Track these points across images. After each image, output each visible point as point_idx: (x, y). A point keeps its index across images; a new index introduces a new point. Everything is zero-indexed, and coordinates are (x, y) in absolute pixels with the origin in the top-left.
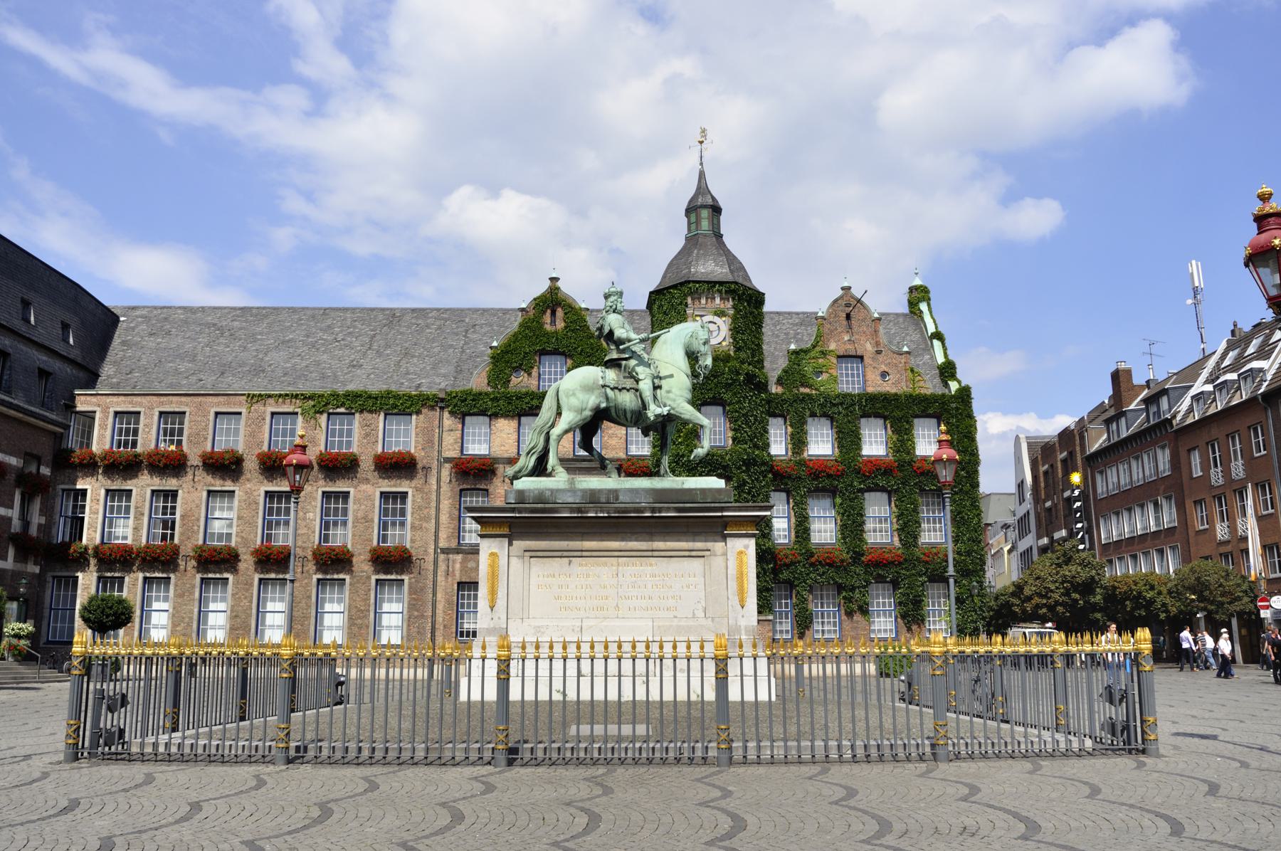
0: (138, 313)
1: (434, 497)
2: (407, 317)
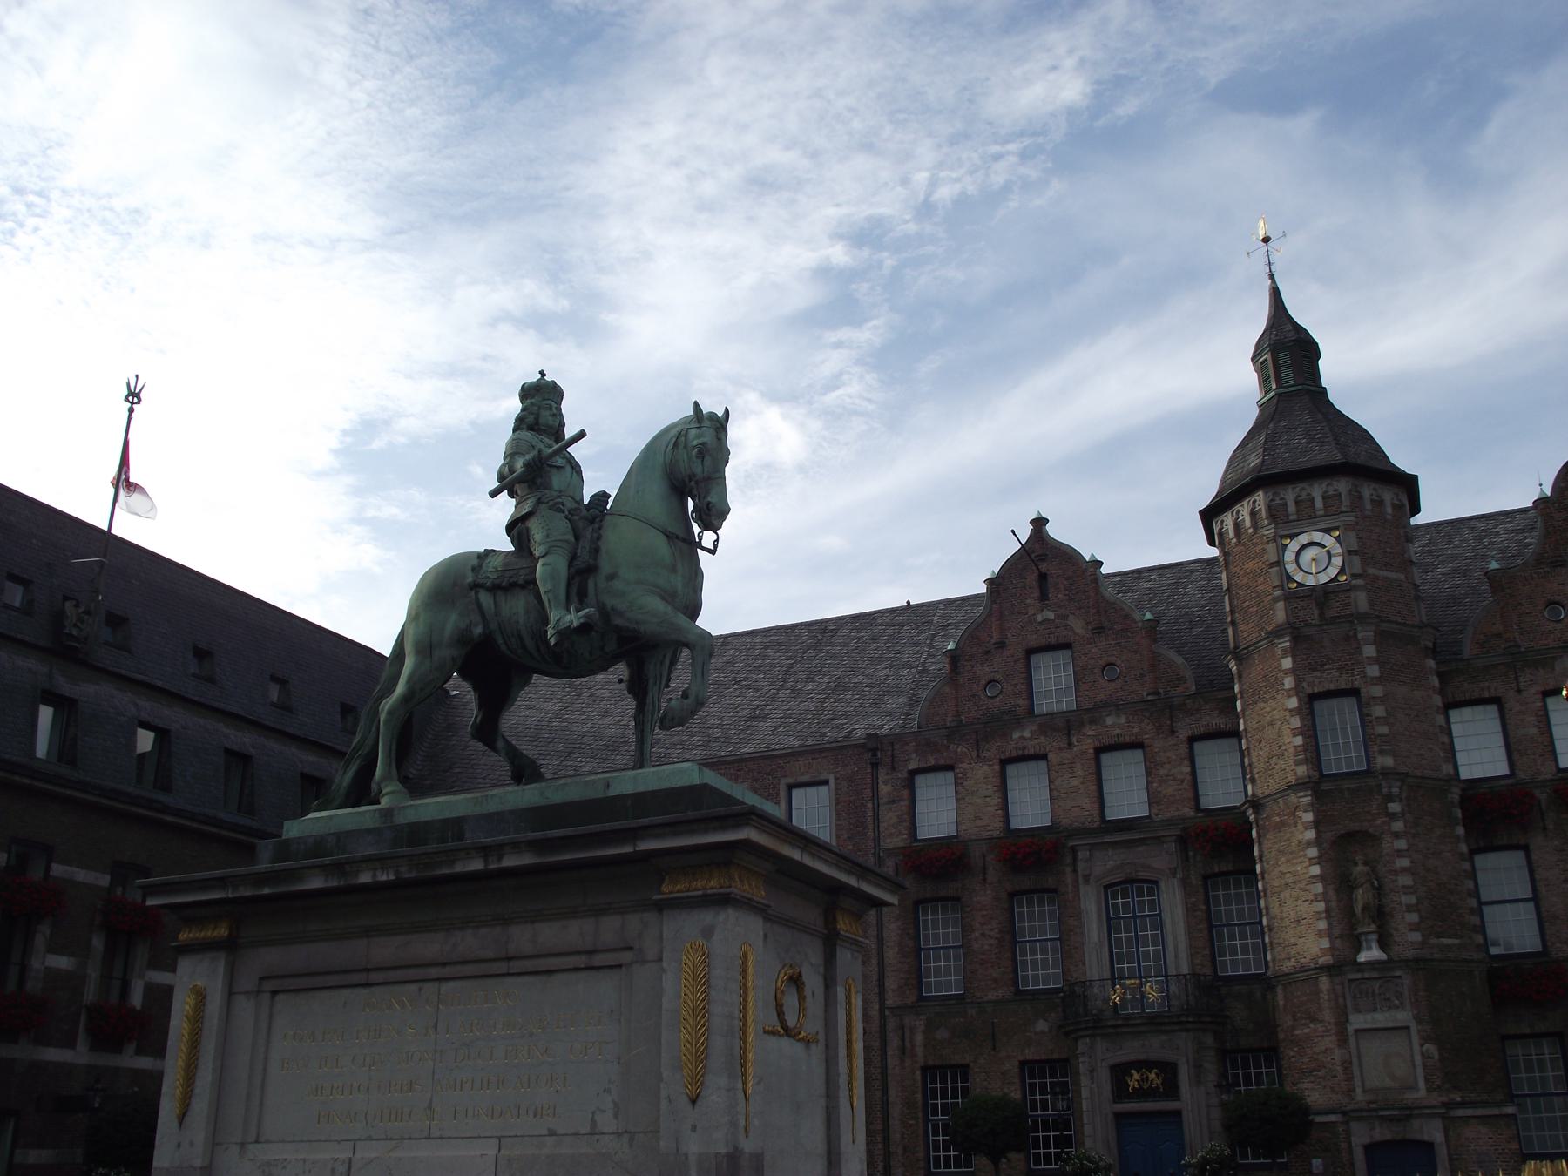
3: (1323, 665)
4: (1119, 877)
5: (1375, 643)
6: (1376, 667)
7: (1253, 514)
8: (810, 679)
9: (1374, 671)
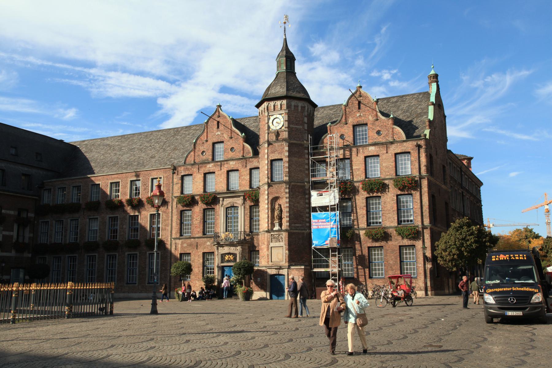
0: (85, 143)
1: (170, 215)
2: (182, 132)
4: (229, 206)
8: (169, 146)
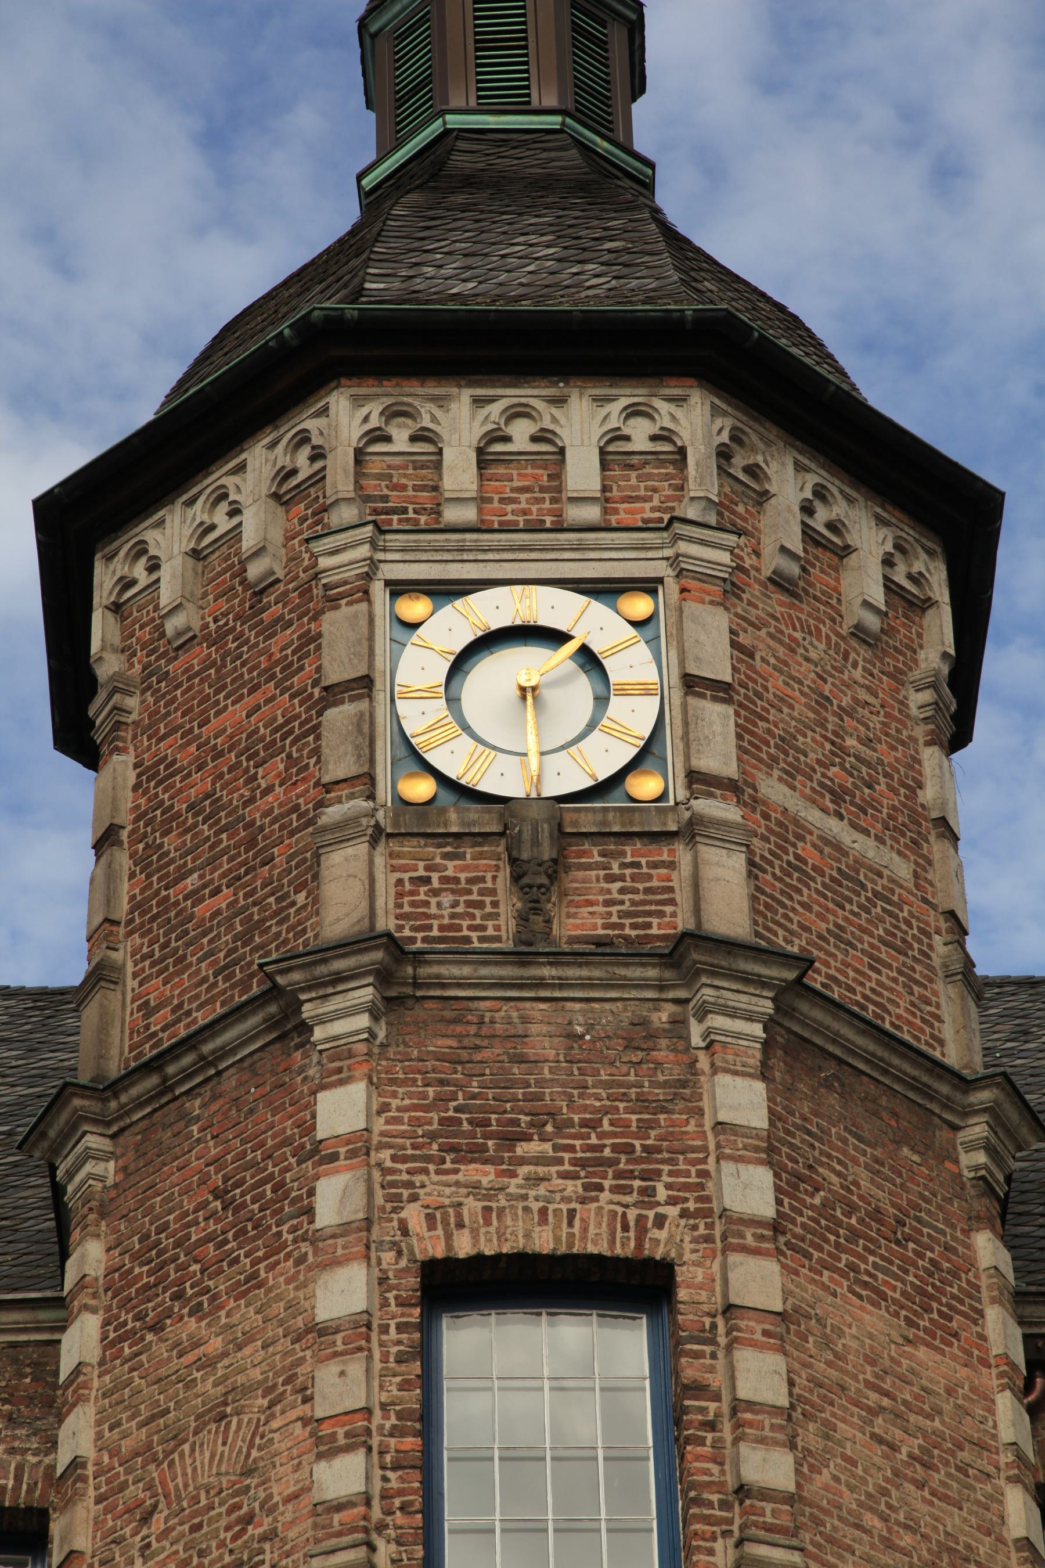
3: (511, 1138)
5: (764, 1074)
6: (762, 1177)
7: (286, 492)
9: (750, 1190)
